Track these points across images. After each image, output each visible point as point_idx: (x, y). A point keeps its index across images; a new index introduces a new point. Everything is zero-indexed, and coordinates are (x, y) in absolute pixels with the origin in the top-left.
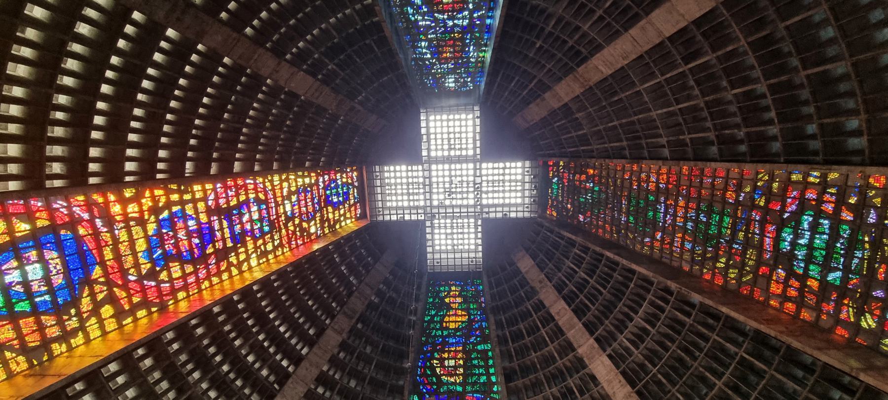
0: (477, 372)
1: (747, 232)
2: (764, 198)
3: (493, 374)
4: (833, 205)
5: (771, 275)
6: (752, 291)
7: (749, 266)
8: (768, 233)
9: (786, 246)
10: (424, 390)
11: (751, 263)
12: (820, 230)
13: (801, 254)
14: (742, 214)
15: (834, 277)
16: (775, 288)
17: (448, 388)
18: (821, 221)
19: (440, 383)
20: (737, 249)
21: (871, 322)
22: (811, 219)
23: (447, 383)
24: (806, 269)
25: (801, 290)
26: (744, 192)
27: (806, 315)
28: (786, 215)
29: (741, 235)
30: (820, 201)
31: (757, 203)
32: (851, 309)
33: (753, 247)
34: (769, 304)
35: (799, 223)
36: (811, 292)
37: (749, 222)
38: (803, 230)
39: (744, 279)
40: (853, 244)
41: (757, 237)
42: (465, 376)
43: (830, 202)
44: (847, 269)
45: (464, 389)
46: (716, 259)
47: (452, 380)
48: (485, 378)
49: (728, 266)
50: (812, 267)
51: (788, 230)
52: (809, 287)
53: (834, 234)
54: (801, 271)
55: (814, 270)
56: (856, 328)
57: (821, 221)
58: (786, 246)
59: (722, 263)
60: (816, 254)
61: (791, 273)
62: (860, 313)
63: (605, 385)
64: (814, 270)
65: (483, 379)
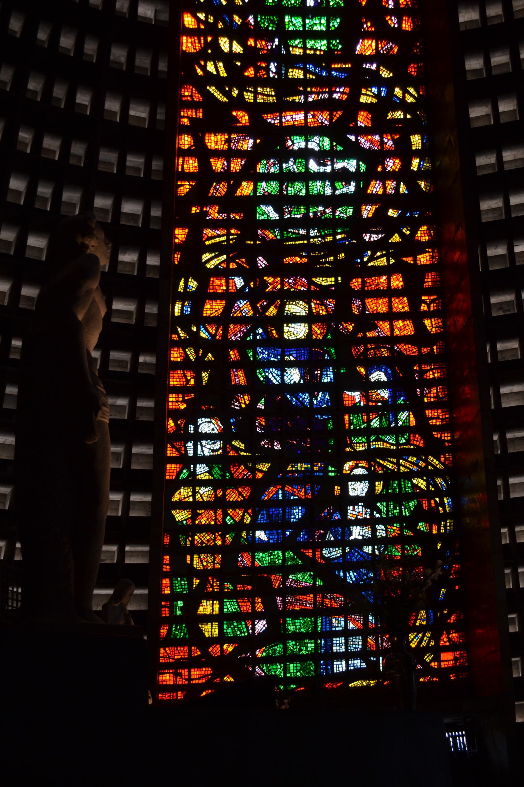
1: (305, 82)
2: (375, 101)
4: (380, 192)
8: (314, 116)
12: (338, 185)
13: (291, 165)
14: (336, 70)
18: (353, 184)
20: (267, 69)
22: (353, 169)
26: (378, 68)
29: (296, 73)
30: (384, 177)
31: (364, 91)
32: (224, 238)
35: (343, 156)
36: (232, 189)
38: (333, 164)
39: (212, 89)
41: (299, 99)
43: (385, 188)
54: (261, 169)
57: (353, 184)
59: (231, 47)
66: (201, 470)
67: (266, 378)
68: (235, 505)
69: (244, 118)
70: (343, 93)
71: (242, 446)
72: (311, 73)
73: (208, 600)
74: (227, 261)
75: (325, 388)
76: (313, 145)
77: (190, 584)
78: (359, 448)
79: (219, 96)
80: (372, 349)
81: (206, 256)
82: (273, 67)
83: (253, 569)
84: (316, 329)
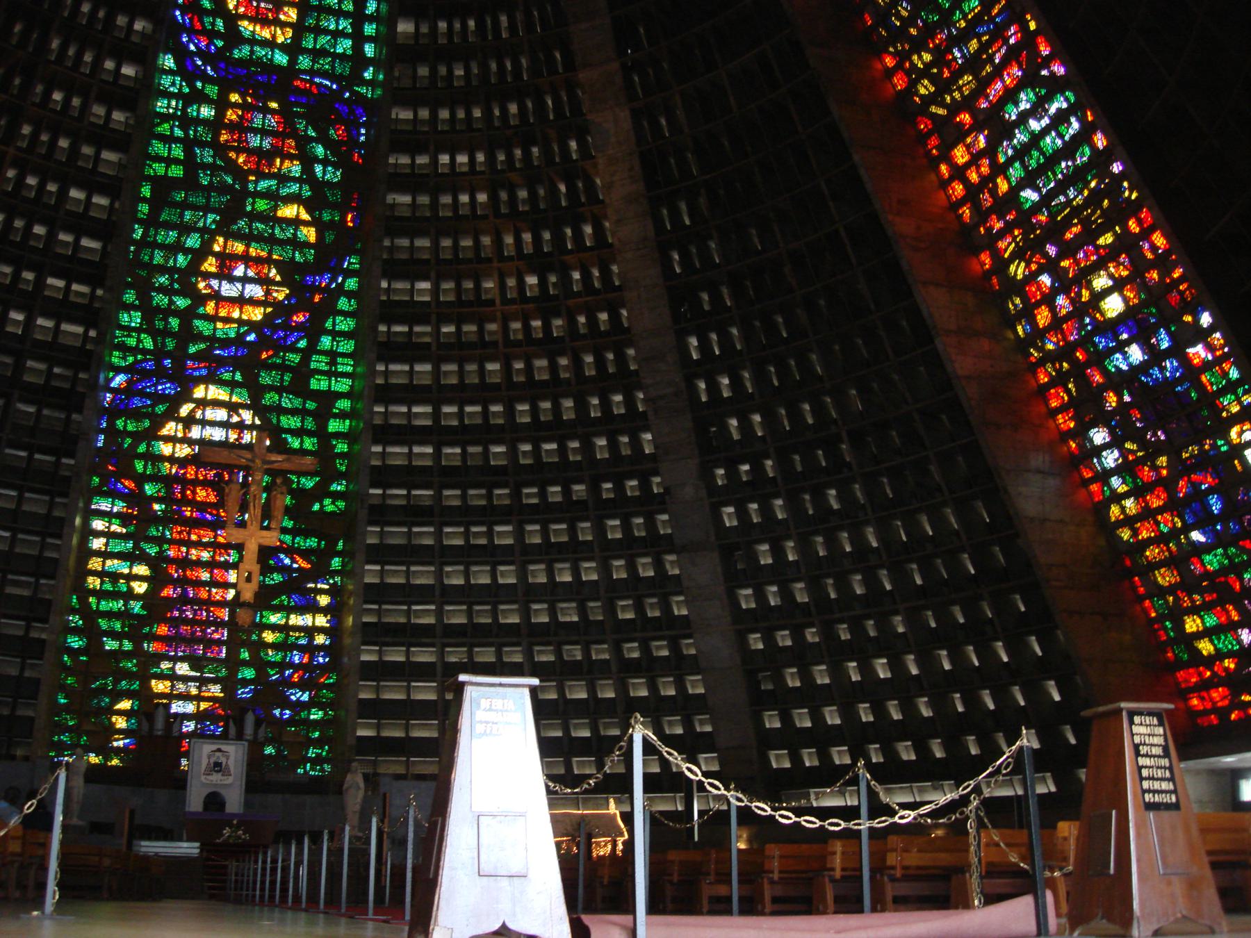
0: (332, 27)
1: (983, 47)
3: (370, 39)
5: (968, 133)
6: (929, 134)
7: (953, 98)
9: (1012, 113)
10: (192, 47)
11: (957, 95)
12: (1062, 129)
13: (1021, 137)
14: (997, 15)
15: (1030, 195)
16: (960, 155)
17: (252, 52)
18: (1073, 120)
19: (234, 37)
20: (955, 59)
21: (1020, 271)
22: (1065, 105)
23: (253, 41)
24: (1010, 162)
25: (987, 182)
27: (966, 212)
28: (1044, 73)
29: (974, 45)
33: (976, 77)
34: (938, 168)
36: (994, 191)
37: (998, 34)
39: (933, 109)
40: (1076, 178)
41: (988, 69)
42: (299, 29)
44: (1045, 200)
45: (293, 61)
46: (919, 46)
47: (266, 34)
48: (348, 43)
49: (925, 73)
50: (1017, 165)
51: (1031, 95)
52: (996, 185)
53: (1069, 150)
54: (1002, 159)
55: (1016, 172)
56: (1001, 265)
57: (1073, 120)
58: (1012, 113)
60: (1035, 154)
61: (991, 151)
62: (1018, 255)
63: (601, 161)
64: (1016, 172)
65: (345, 45)
66: (1115, 482)
67: (1116, 367)
68: (1160, 510)
69: (966, 118)
70: (1015, 33)
71: (1135, 447)
72: (984, 34)
73: (1188, 615)
74: (1028, 266)
75: (1168, 354)
76: (1024, 106)
77: (1167, 602)
78: (1235, 409)
79: (941, 112)
80: (1186, 290)
81: (1012, 268)
82: (958, 54)
83: (1207, 575)
84: (1128, 294)
